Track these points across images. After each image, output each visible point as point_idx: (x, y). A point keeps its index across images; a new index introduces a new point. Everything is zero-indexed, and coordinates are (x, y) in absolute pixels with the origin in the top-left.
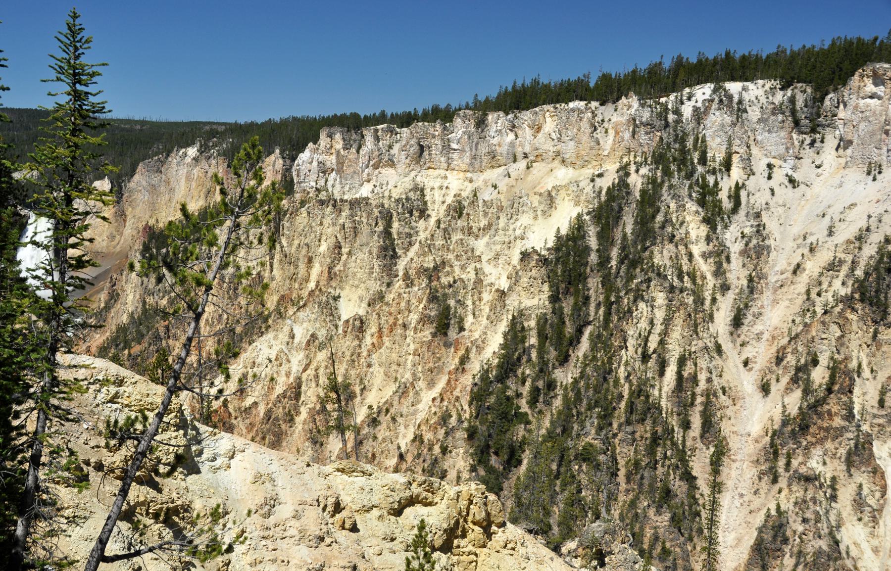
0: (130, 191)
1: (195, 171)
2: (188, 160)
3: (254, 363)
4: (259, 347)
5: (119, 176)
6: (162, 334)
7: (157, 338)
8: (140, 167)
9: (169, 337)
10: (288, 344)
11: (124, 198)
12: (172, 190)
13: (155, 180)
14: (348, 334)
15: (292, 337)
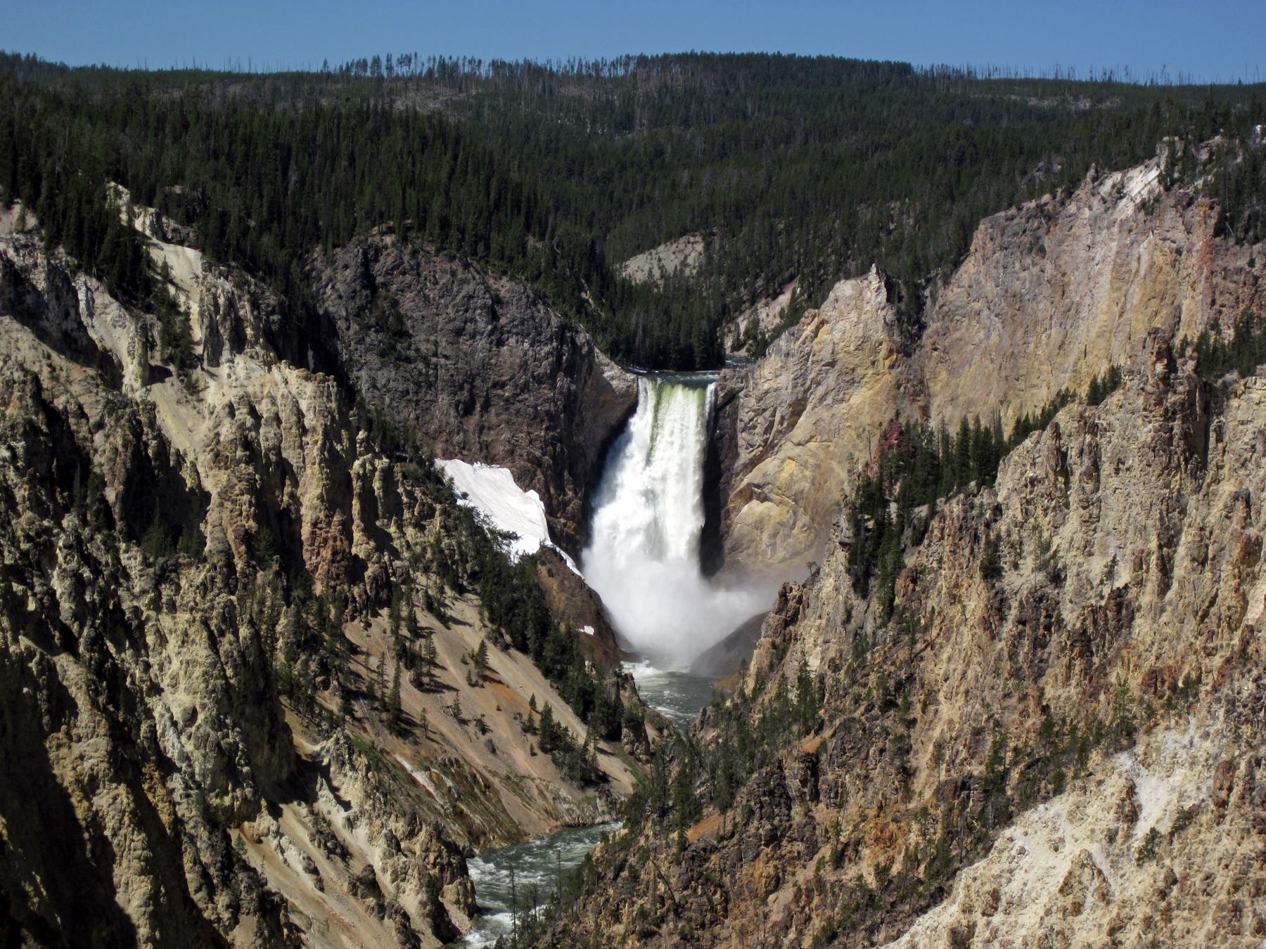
0: (948, 316)
1: (1143, 249)
2: (1126, 209)
3: (995, 895)
4: (1019, 843)
5: (918, 267)
6: (793, 784)
7: (778, 795)
8: (980, 236)
9: (815, 797)
10: (1111, 838)
11: (927, 339)
12: (1070, 313)
13: (1022, 280)
14: (1230, 812)
15: (1132, 816)
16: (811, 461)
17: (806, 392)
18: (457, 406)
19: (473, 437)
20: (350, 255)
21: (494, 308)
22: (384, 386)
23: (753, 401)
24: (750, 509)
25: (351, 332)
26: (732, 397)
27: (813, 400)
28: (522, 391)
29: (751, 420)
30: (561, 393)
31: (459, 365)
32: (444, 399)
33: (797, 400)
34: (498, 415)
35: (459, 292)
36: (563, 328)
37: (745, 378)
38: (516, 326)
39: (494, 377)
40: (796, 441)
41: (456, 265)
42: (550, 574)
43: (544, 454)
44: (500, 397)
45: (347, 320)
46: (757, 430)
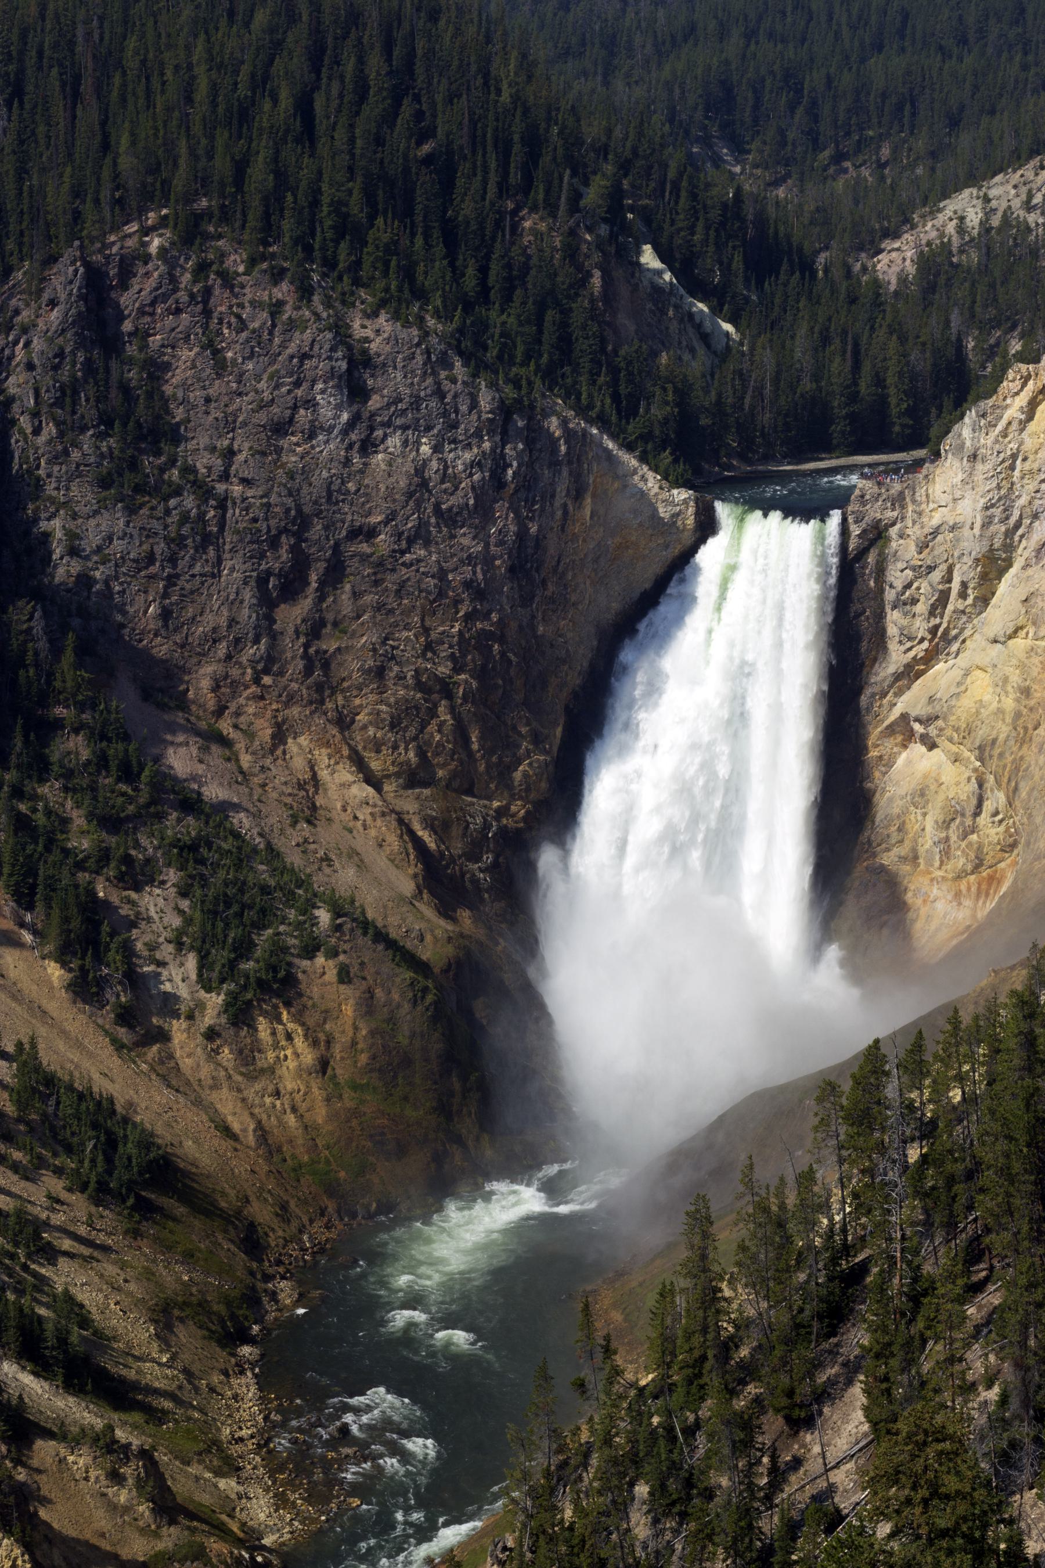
16: (1015, 678)
17: (1010, 533)
18: (262, 581)
19: (292, 648)
20: (65, 279)
21: (355, 378)
22: (99, 549)
23: (913, 548)
24: (909, 762)
25: (42, 439)
26: (877, 534)
27: (1024, 551)
28: (411, 542)
29: (908, 586)
30: (501, 543)
31: (274, 499)
32: (235, 570)
33: (991, 550)
34: (356, 595)
35: (283, 346)
36: (505, 411)
37: (898, 502)
38: (404, 412)
39: (349, 516)
40: (992, 636)
41: (283, 291)
42: (344, 976)
43: (457, 669)
44: (364, 558)
45: (35, 414)
46: (921, 608)
